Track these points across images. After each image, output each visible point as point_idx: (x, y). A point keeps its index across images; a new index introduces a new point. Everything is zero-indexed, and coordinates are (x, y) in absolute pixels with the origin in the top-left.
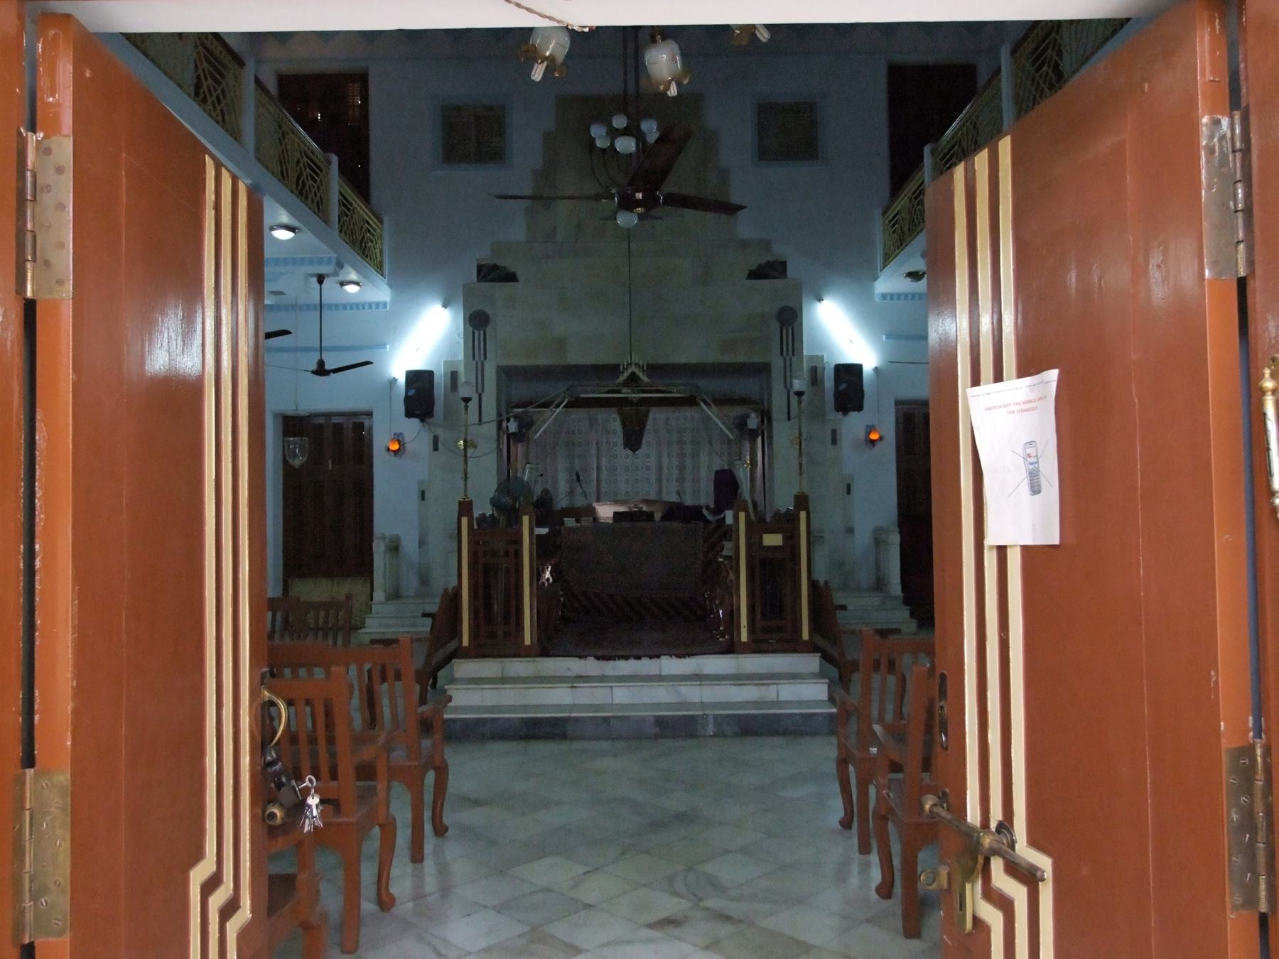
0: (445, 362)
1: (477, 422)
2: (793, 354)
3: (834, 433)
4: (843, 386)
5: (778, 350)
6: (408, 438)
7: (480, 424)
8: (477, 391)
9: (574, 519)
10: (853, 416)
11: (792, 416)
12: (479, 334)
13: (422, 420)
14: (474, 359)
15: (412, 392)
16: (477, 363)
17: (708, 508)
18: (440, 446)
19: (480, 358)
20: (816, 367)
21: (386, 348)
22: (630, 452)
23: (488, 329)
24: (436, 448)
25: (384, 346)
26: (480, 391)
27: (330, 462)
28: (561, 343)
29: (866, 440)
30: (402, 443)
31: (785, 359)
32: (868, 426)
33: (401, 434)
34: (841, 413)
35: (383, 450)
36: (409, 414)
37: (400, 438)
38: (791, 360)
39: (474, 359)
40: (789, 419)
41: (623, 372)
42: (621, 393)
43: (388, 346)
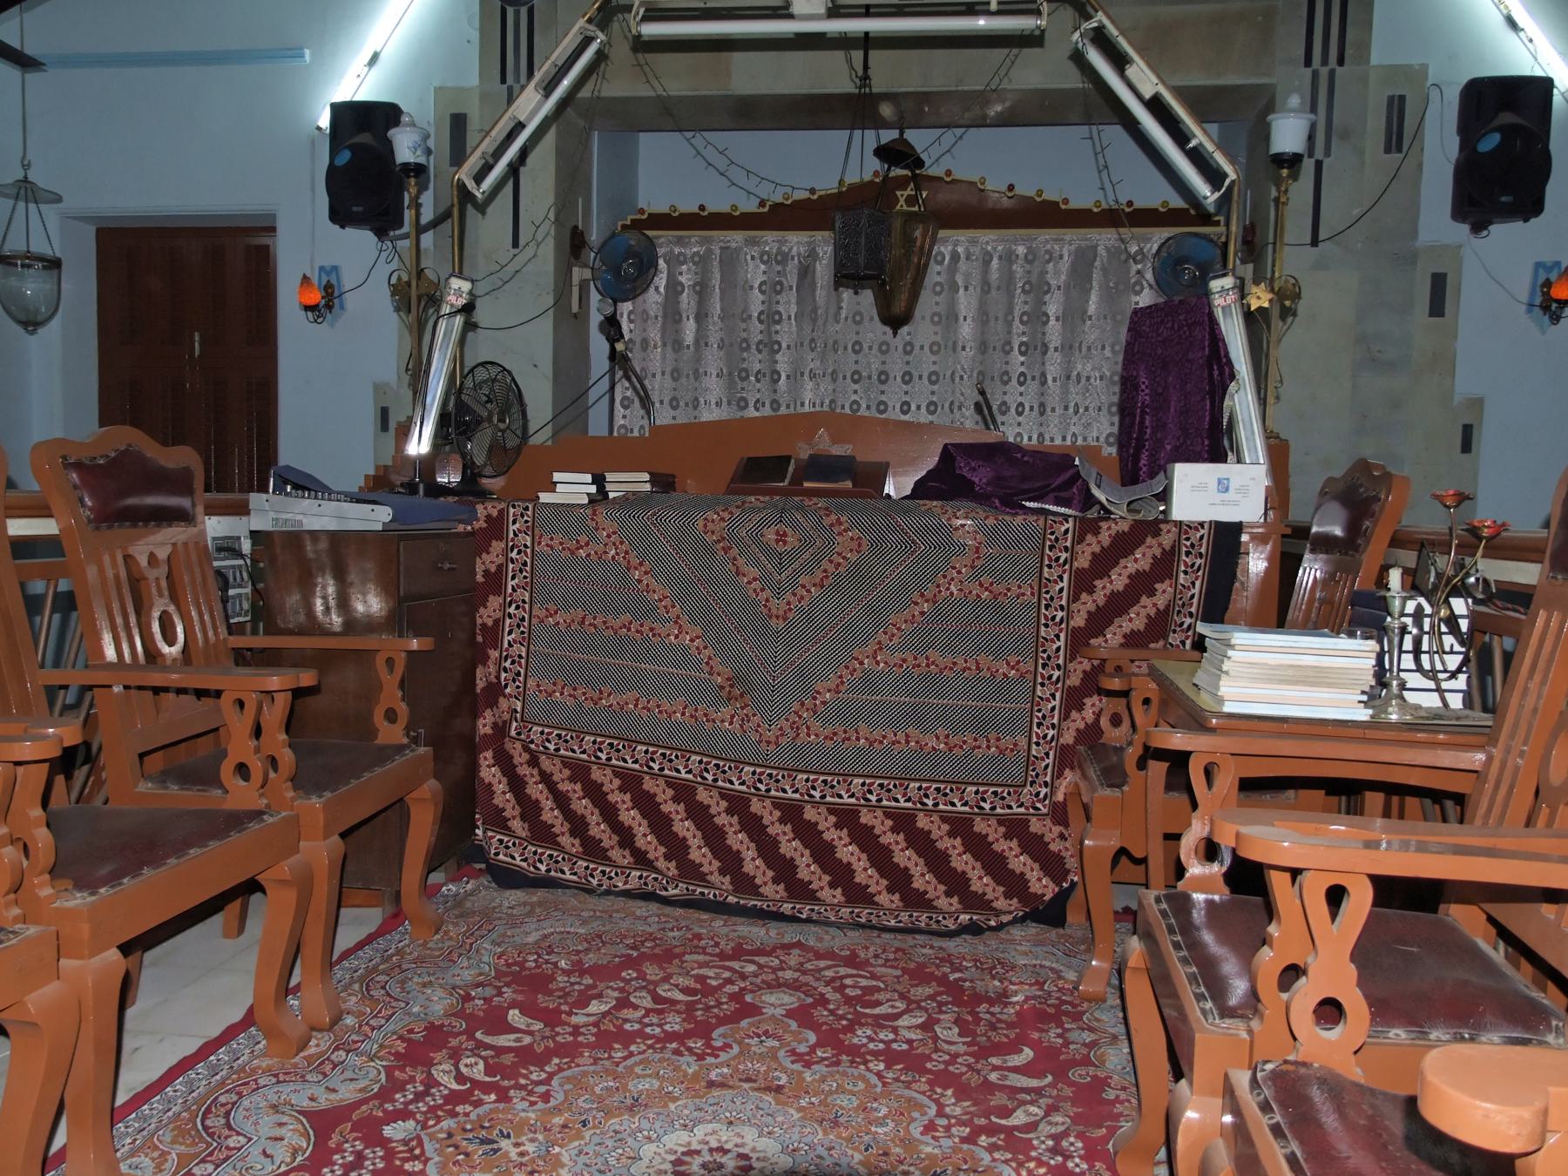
0: (438, 90)
2: (1341, 62)
3: (1439, 283)
4: (1490, 143)
5: (1301, 52)
6: (348, 280)
9: (588, 478)
10: (1504, 233)
11: (1322, 235)
12: (517, 13)
13: (381, 233)
14: (503, 81)
15: (344, 157)
17: (1091, 453)
20: (1402, 98)
21: (303, 56)
22: (888, 330)
25: (295, 52)
27: (197, 337)
29: (1531, 305)
30: (336, 294)
31: (1315, 74)
32: (1538, 265)
33: (335, 269)
34: (1465, 228)
36: (340, 216)
37: (334, 282)
38: (1332, 73)
39: (503, 81)
42: (791, 17)
43: (307, 52)
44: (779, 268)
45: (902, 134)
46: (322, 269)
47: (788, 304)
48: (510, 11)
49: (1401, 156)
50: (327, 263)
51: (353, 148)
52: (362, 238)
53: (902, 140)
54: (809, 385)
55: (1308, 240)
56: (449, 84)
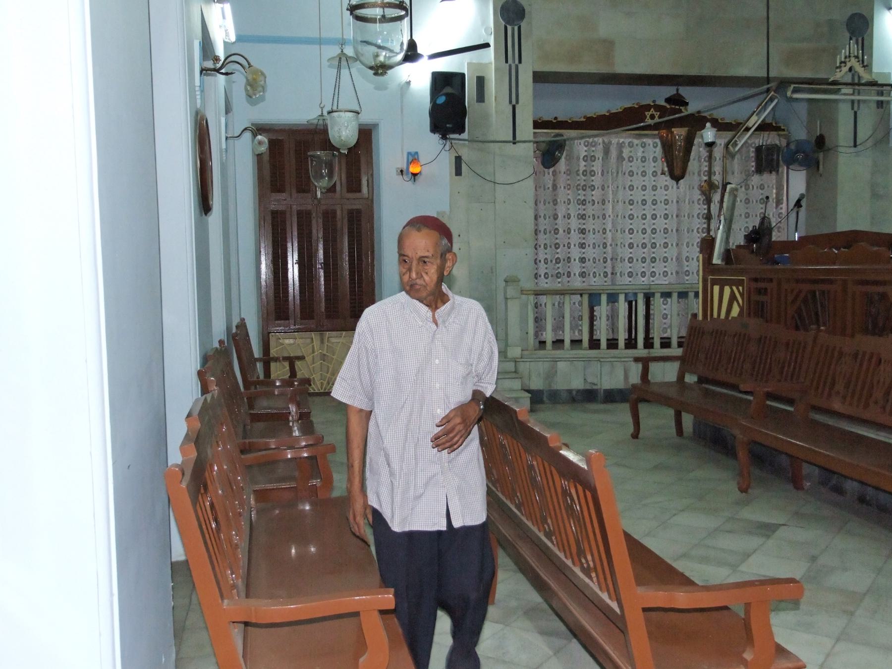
1: (511, 139)
7: (514, 143)
8: (510, 102)
11: (858, 143)
13: (444, 137)
14: (507, 61)
15: (441, 100)
16: (510, 66)
18: (464, 168)
19: (514, 62)
23: (523, 24)
24: (458, 172)
26: (514, 102)
28: (608, 45)
33: (417, 153)
35: (394, 173)
39: (507, 61)
40: (855, 146)
41: (840, 67)
44: (594, 149)
45: (677, 90)
46: (409, 154)
47: (597, 166)
48: (509, 28)
49: (882, 110)
50: (413, 150)
51: (447, 95)
52: (436, 137)
53: (678, 94)
54: (610, 206)
55: (852, 144)
56: (474, 62)
